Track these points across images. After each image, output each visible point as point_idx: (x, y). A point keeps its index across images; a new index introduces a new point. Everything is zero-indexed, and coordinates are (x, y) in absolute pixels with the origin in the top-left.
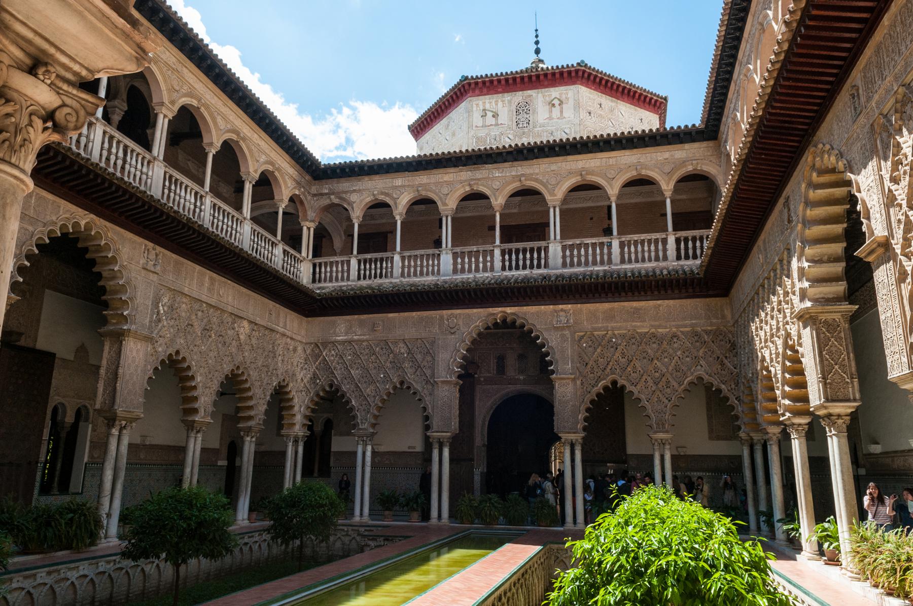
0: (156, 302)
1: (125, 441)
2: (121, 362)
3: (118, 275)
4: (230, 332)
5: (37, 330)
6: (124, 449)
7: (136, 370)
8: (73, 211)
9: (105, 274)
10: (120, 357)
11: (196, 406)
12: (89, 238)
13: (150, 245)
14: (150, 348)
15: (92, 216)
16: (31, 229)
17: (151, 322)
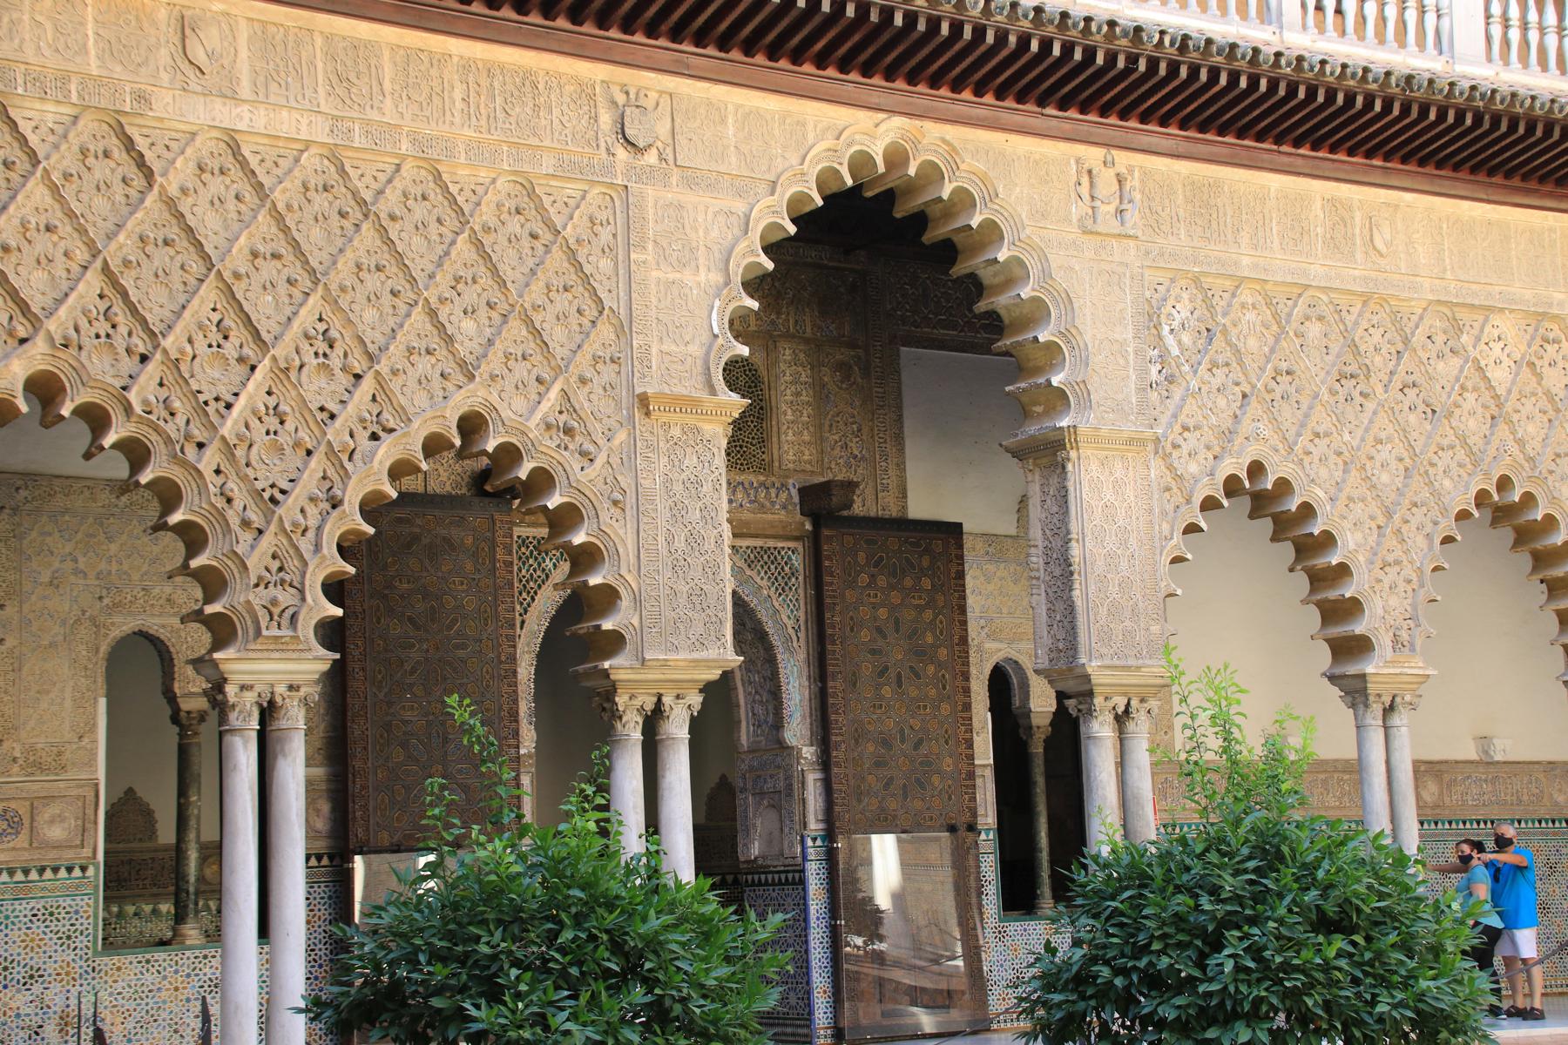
0: (1151, 319)
1: (1141, 757)
2: (1074, 526)
3: (1017, 271)
4: (1447, 368)
5: (901, 466)
6: (1143, 783)
7: (1124, 543)
8: (841, 124)
9: (986, 275)
10: (1066, 512)
11: (1359, 628)
12: (912, 188)
13: (1093, 155)
14: (1156, 469)
15: (898, 121)
16: (740, 207)
17: (1140, 390)
